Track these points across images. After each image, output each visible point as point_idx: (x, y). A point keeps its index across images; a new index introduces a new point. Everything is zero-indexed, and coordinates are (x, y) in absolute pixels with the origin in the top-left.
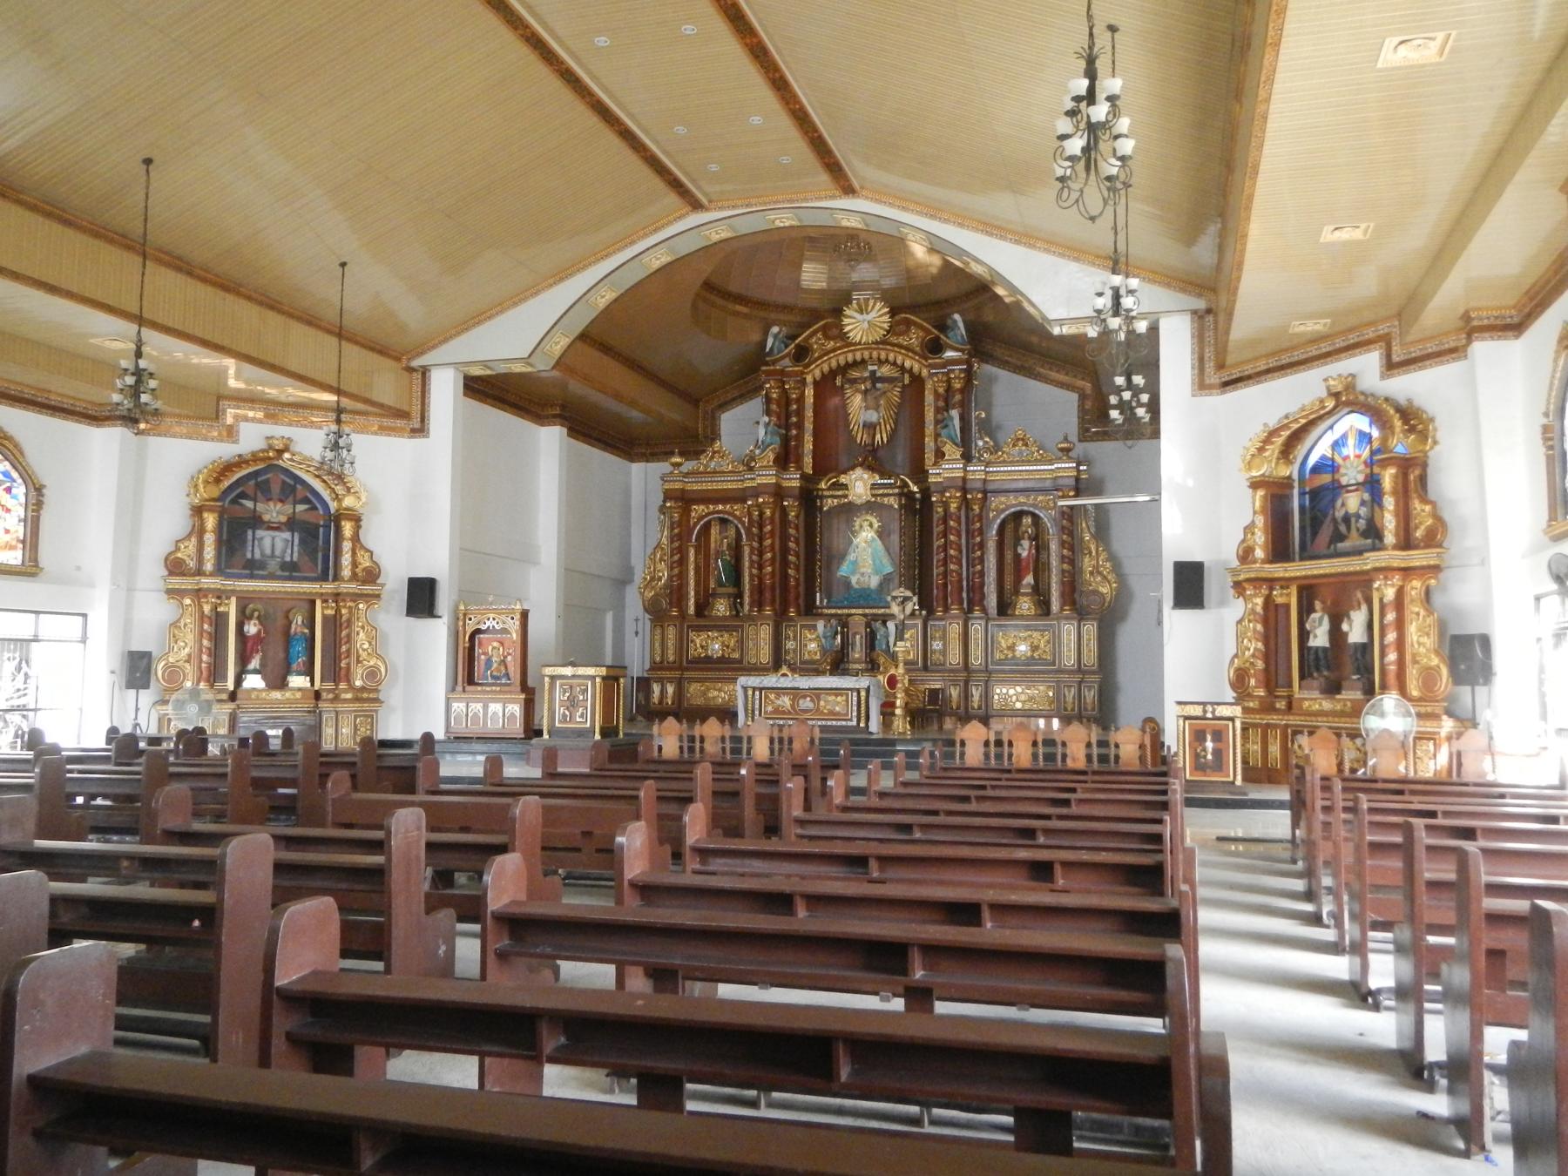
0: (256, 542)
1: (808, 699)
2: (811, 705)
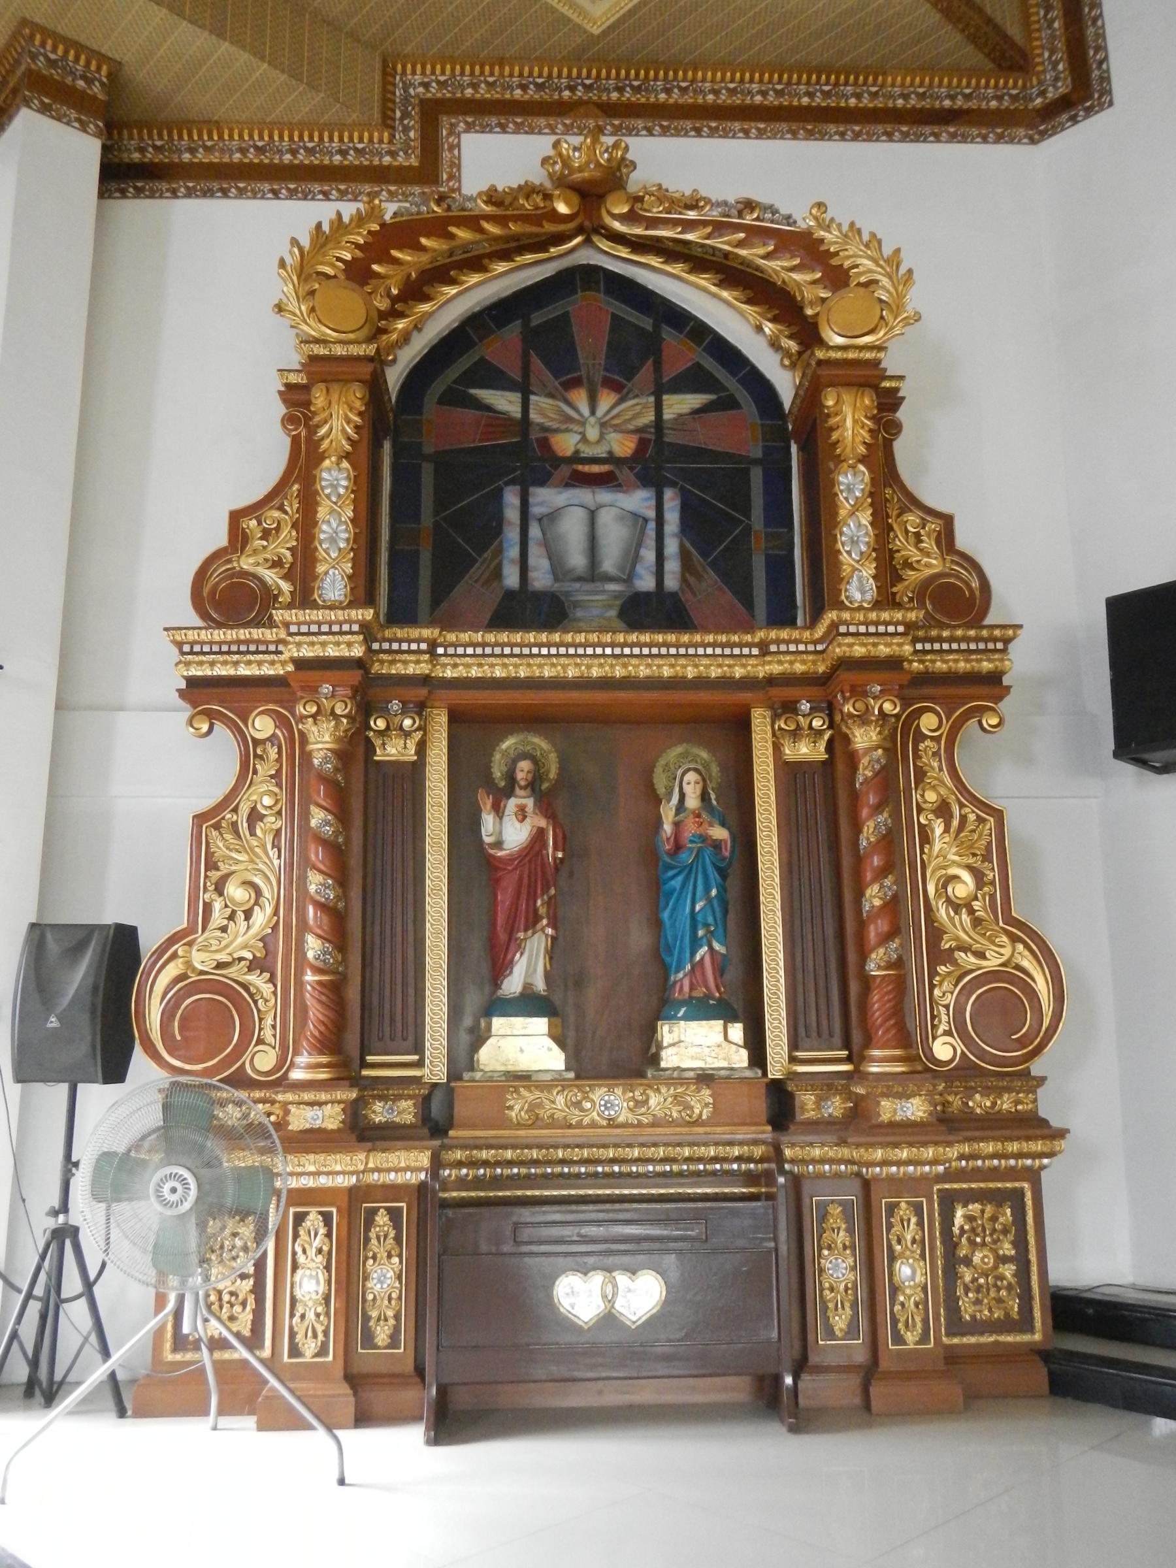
0: (535, 531)
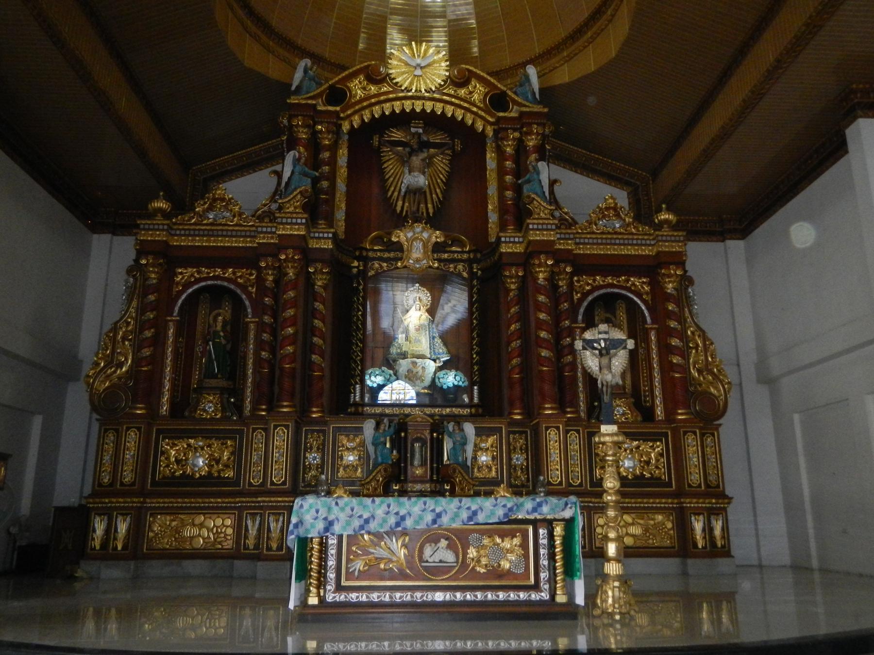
1: (443, 543)
2: (450, 557)
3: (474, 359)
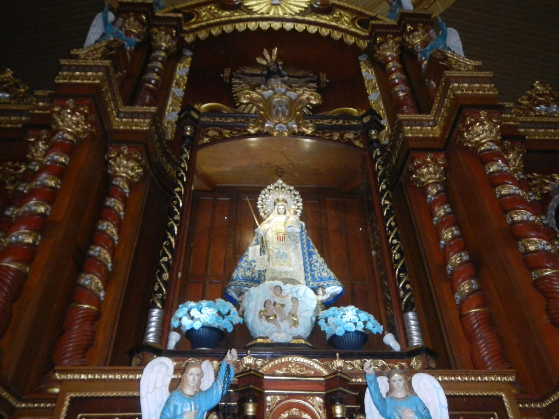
3: (397, 262)
